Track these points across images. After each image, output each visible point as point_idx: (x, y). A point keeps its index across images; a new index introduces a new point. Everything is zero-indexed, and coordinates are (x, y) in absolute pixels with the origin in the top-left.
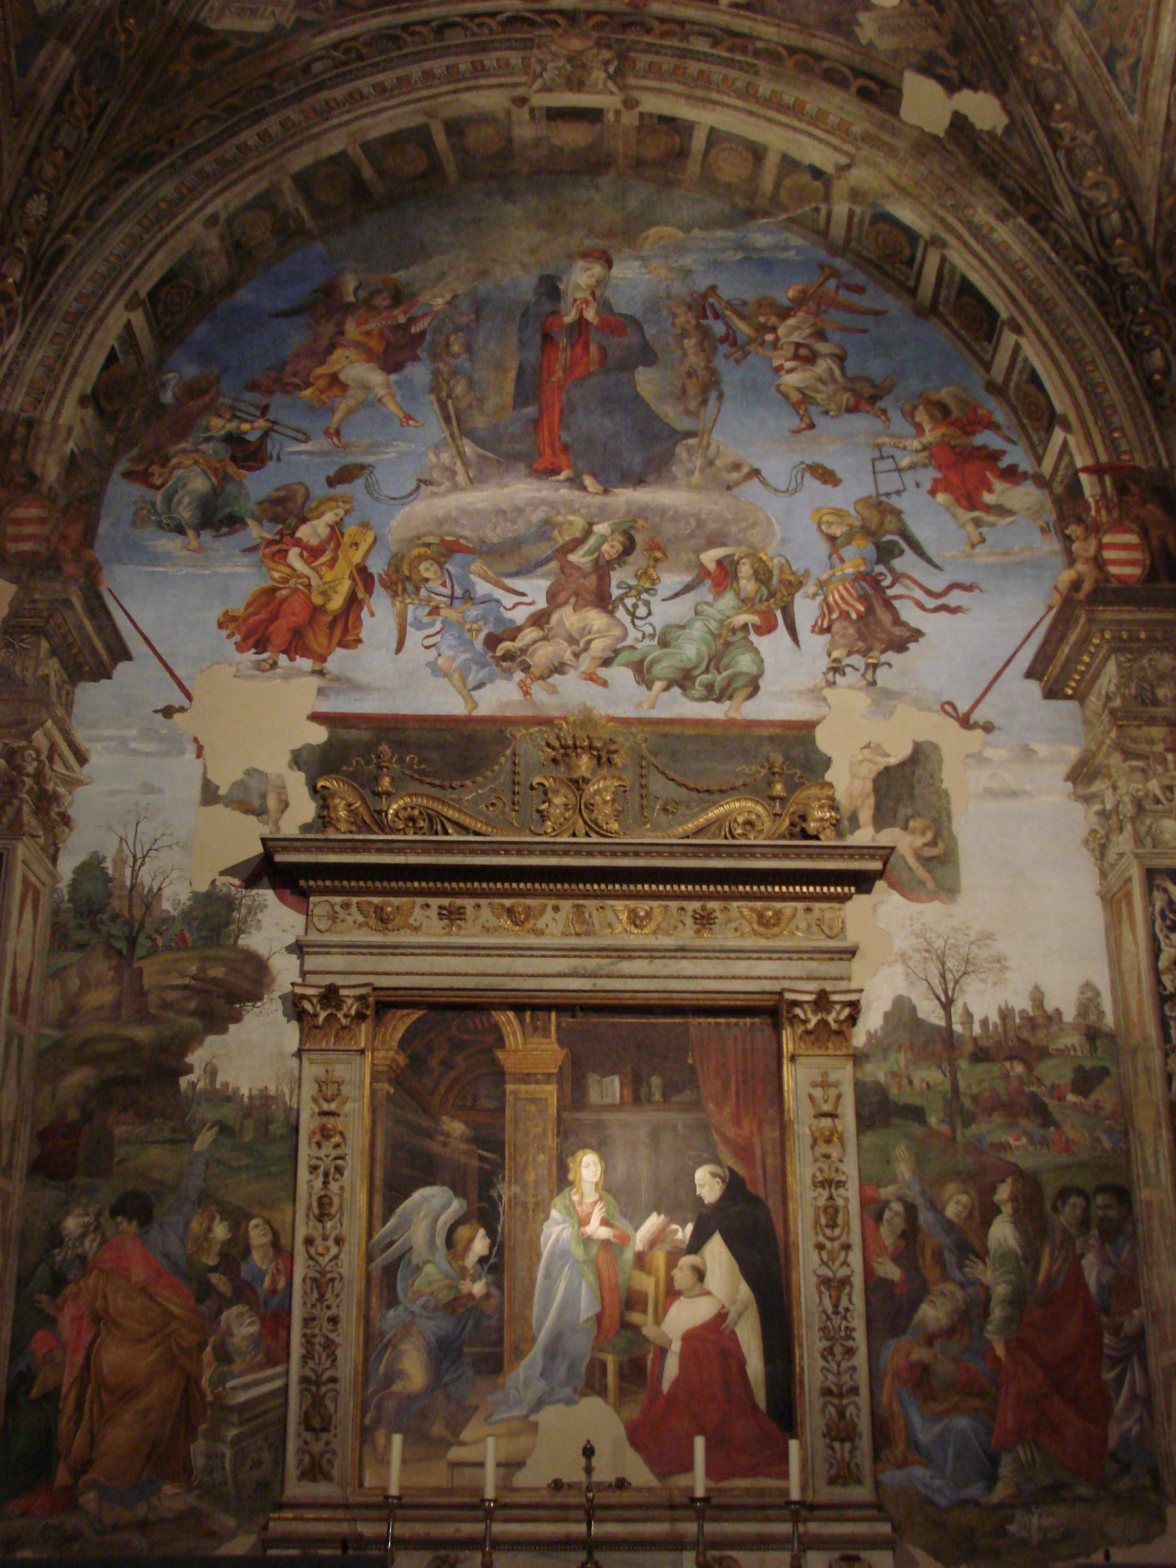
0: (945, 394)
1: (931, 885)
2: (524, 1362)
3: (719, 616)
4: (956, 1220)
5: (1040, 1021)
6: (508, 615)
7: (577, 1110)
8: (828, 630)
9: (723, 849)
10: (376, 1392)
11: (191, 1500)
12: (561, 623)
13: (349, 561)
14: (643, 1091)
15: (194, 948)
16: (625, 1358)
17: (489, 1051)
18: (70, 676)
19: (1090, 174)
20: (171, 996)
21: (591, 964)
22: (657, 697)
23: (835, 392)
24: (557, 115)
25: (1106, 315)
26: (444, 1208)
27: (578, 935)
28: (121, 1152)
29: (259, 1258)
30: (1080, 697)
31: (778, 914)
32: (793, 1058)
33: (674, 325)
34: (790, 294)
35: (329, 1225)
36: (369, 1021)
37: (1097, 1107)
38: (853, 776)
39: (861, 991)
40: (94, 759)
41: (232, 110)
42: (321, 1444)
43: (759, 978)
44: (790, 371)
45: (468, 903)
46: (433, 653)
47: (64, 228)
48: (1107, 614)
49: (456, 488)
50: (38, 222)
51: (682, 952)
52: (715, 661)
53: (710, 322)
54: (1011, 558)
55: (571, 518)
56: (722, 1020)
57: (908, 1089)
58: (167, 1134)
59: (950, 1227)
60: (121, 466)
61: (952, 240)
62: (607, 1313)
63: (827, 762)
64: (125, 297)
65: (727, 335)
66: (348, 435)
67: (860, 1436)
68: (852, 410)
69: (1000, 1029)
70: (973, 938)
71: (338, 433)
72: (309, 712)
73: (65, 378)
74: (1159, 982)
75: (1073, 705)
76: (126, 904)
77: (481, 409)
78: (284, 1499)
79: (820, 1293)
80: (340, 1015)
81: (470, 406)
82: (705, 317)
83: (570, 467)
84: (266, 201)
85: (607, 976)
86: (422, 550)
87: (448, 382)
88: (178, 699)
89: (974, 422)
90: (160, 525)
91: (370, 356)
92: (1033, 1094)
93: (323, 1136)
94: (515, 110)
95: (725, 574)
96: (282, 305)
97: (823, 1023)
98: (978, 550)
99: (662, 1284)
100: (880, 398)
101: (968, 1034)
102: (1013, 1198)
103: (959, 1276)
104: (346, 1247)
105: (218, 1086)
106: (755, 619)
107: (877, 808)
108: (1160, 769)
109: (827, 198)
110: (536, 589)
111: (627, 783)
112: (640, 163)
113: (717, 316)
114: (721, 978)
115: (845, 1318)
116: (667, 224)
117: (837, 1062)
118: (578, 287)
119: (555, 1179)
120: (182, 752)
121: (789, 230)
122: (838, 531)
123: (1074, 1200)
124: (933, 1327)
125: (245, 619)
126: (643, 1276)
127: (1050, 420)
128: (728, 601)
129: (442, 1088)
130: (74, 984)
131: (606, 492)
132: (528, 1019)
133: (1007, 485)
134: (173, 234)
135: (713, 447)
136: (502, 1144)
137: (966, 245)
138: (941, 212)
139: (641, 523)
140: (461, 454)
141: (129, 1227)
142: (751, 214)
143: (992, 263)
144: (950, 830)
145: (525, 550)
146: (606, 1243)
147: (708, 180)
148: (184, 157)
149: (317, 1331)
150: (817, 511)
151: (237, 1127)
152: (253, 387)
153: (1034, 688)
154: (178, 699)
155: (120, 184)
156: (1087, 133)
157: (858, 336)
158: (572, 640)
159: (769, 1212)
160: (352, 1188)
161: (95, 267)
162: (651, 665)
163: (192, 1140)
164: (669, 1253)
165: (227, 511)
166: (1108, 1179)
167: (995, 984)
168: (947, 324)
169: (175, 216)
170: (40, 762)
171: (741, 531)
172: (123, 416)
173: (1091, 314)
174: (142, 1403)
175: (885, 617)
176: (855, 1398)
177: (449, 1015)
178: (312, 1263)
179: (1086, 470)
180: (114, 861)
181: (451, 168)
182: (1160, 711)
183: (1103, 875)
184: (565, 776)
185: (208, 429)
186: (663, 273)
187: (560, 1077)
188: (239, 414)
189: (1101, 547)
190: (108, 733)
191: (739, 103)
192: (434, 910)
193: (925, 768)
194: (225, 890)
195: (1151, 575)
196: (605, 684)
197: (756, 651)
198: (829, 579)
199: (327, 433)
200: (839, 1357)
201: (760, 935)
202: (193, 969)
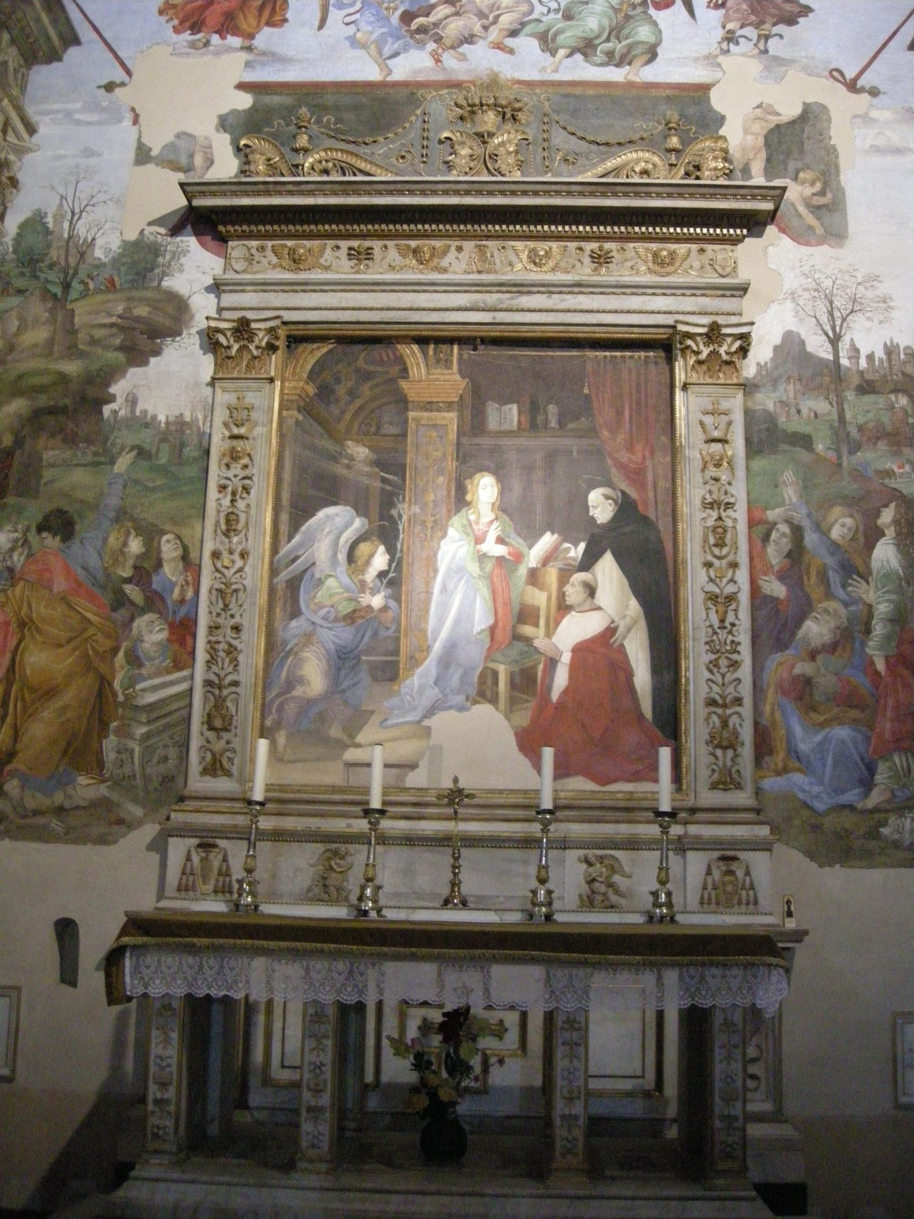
1: (819, 230)
2: (419, 671)
4: (840, 541)
7: (476, 435)
8: (723, 5)
9: (618, 188)
10: (278, 695)
11: (103, 790)
14: (540, 418)
15: (122, 290)
16: (516, 669)
17: (393, 380)
18: (26, 60)
20: (99, 333)
21: (492, 299)
22: (560, 63)
27: (479, 272)
28: (47, 474)
29: (171, 571)
31: (672, 255)
32: (685, 387)
35: (235, 539)
36: (279, 352)
38: (746, 132)
39: (752, 324)
40: (42, 130)
42: (222, 743)
43: (653, 312)
45: (376, 245)
46: (352, 28)
51: (578, 287)
52: (616, 32)
56: (618, 354)
57: (796, 417)
58: (89, 458)
59: (835, 547)
62: (500, 623)
67: (743, 744)
72: (236, 82)
76: (62, 252)
78: (186, 793)
79: (708, 609)
80: (252, 347)
85: (506, 310)
88: (119, 75)
93: (232, 458)
97: (714, 354)
99: (554, 598)
101: (854, 368)
102: (896, 522)
103: (841, 593)
104: (250, 561)
105: (138, 414)
107: (769, 160)
114: (616, 312)
115: (730, 632)
117: (729, 391)
119: (453, 500)
120: (120, 121)
124: (816, 643)
126: (536, 591)
129: (348, 416)
130: (13, 325)
132: (431, 352)
136: (403, 467)
141: (52, 541)
144: (838, 182)
146: (500, 560)
149: (221, 639)
151: (154, 450)
154: (120, 75)
158: (481, 15)
160: (258, 506)
162: (556, 35)
163: (112, 462)
164: (561, 570)
167: (881, 322)
174: (60, 702)
176: (738, 709)
177: (358, 348)
178: (218, 575)
180: (55, 217)
184: (474, 130)
190: (55, 107)
193: (814, 125)
194: (152, 238)
196: (511, 52)
197: (655, 24)
200: (724, 670)
202: (120, 309)
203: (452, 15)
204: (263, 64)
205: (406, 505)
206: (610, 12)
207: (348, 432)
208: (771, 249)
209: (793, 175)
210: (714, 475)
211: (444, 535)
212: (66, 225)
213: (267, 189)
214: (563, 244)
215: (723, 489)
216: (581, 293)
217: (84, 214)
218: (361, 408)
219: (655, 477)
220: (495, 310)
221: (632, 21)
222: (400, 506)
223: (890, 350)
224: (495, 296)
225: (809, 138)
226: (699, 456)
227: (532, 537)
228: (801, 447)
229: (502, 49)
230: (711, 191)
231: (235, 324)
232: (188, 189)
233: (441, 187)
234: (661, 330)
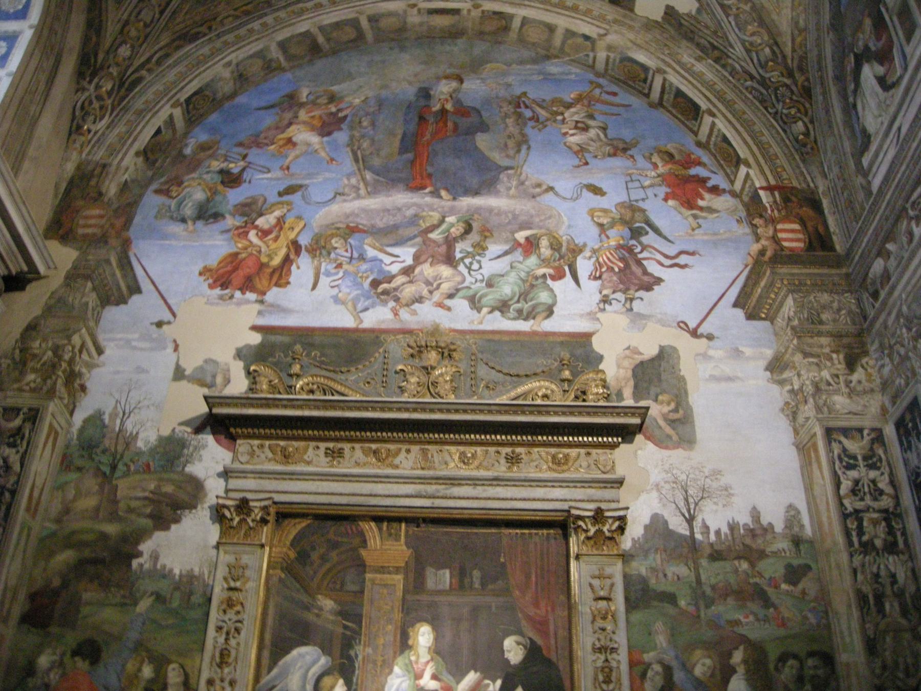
0: (670, 147)
1: (675, 438)
3: (527, 269)
4: (702, 678)
5: (759, 532)
6: (387, 268)
7: (417, 594)
8: (600, 277)
9: (526, 408)
12: (422, 273)
13: (287, 239)
14: (467, 581)
15: (155, 472)
17: (355, 550)
19: (750, 27)
20: (134, 504)
21: (431, 489)
22: (484, 317)
23: (601, 146)
25: (766, 108)
26: (315, 662)
27: (423, 469)
30: (771, 319)
31: (566, 457)
32: (577, 557)
33: (500, 112)
34: (572, 96)
36: (270, 525)
37: (804, 592)
38: (619, 366)
39: (627, 508)
40: (108, 352)
41: (247, 13)
44: (572, 135)
45: (346, 446)
46: (336, 291)
47: (142, 66)
48: (784, 270)
49: (359, 197)
51: (496, 481)
52: (524, 296)
53: (523, 110)
54: (719, 237)
55: (431, 213)
56: (526, 531)
57: (663, 580)
60: (155, 186)
61: (668, 69)
63: (600, 358)
68: (610, 155)
69: (730, 538)
70: (707, 474)
71: (288, 168)
72: (250, 325)
73: (129, 142)
74: (842, 504)
75: (767, 324)
80: (249, 520)
81: (371, 154)
82: (520, 107)
83: (432, 185)
84: (260, 54)
85: (442, 498)
86: (334, 231)
89: (689, 162)
90: (172, 218)
91: (313, 129)
92: (757, 584)
93: (228, 605)
94: (409, 9)
95: (531, 245)
96: (263, 104)
97: (599, 532)
98: (696, 232)
100: (630, 149)
101: (706, 541)
102: (745, 662)
106: (551, 271)
107: (636, 387)
108: (828, 364)
109: (593, 50)
110: (406, 254)
111: (462, 371)
113: (527, 107)
116: (498, 62)
118: (442, 93)
119: (398, 644)
120: (165, 348)
123: (791, 662)
125: (217, 270)
127: (738, 161)
128: (533, 260)
131: (454, 199)
133: (713, 196)
134: (204, 71)
136: (361, 616)
137: (678, 72)
138: (662, 57)
139: (476, 216)
140: (364, 179)
142: (548, 57)
143: (695, 82)
144: (687, 402)
145: (400, 231)
147: (522, 40)
151: (168, 596)
152: (240, 144)
153: (739, 313)
154: (167, 316)
155: (178, 48)
158: (428, 283)
159: (559, 671)
161: (159, 87)
162: (481, 298)
165: (213, 211)
166: (815, 647)
167: (724, 506)
168: (669, 111)
171: (541, 221)
172: (160, 161)
173: (757, 108)
175: (638, 271)
177: (329, 523)
179: (762, 188)
180: (110, 415)
181: (369, 36)
182: (823, 328)
183: (796, 432)
185: (209, 167)
187: (406, 570)
190: (119, 336)
191: (542, 6)
192: (322, 450)
193: (668, 362)
194: (180, 435)
195: (810, 247)
196: (449, 309)
197: (552, 290)
198: (600, 248)
199: (281, 168)
201: (554, 470)
202: (152, 487)
204: (271, 313)
205: (362, 647)
206: (520, 282)
207: (319, 588)
208: (639, 452)
209: (654, 398)
210: (601, 626)
211: (391, 671)
212: (118, 422)
214: (484, 448)
215: (608, 638)
216: (498, 485)
217: (132, 415)
218: (329, 570)
219: (556, 627)
220: (434, 497)
222: (356, 647)
223: (733, 527)
224: (434, 487)
226: (589, 610)
227: (459, 675)
228: (668, 602)
229: (442, 307)
230: (594, 410)
231: (237, 502)
232: (210, 400)
234: (559, 514)
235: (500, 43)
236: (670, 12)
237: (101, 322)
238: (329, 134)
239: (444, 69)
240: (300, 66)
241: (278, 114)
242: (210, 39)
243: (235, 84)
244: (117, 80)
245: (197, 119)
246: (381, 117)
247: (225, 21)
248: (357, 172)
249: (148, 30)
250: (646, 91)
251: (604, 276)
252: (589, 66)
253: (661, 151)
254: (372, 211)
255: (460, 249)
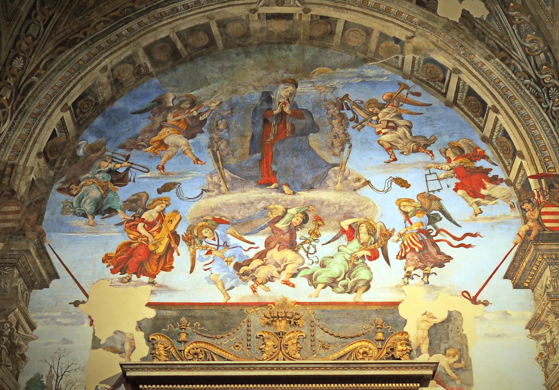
3: (350, 252)
8: (405, 257)
9: (351, 365)
12: (272, 257)
19: (529, 36)
22: (319, 292)
23: (407, 143)
24: (270, 17)
38: (418, 328)
40: (39, 328)
41: (116, 18)
47: (32, 74)
49: (220, 193)
50: (18, 71)
52: (348, 274)
54: (496, 221)
55: (277, 206)
60: (57, 186)
61: (463, 70)
64: (61, 106)
65: (354, 117)
66: (168, 169)
68: (414, 152)
71: (163, 168)
72: (146, 303)
77: (233, 155)
81: (228, 154)
82: (343, 109)
83: (276, 182)
84: (130, 60)
86: (204, 223)
87: (217, 143)
88: (82, 297)
90: (75, 213)
94: (251, 14)
96: (137, 108)
98: (479, 216)
100: (429, 145)
106: (368, 253)
107: (430, 344)
109: (402, 52)
112: (311, 38)
113: (348, 109)
116: (324, 66)
118: (281, 96)
120: (83, 323)
121: (383, 67)
122: (409, 209)
127: (515, 153)
128: (355, 244)
131: (294, 193)
134: (85, 75)
135: (347, 171)
137: (470, 72)
138: (458, 57)
140: (223, 177)
142: (365, 61)
143: (483, 80)
144: (468, 355)
145: (254, 222)
148: (92, 40)
150: (398, 200)
152: (123, 147)
154: (82, 297)
155: (60, 53)
156: (527, 16)
157: (418, 116)
158: (277, 265)
165: (108, 206)
169: (87, 67)
170: (12, 329)
172: (58, 162)
173: (533, 103)
180: (47, 377)
181: (220, 43)
186: (322, 89)
188: (115, 160)
189: (541, 214)
190: (46, 314)
191: (360, 9)
196: (293, 286)
197: (369, 269)
199: (158, 168)
203: (261, 265)
206: (346, 263)
212: (54, 382)
213: (167, 367)
217: (64, 376)
221: (356, 267)
225: (451, 331)
229: (288, 285)
232: (124, 367)
233: (259, 366)
235: (327, 47)
236: (466, 16)
237: (30, 303)
238: (193, 136)
239: (281, 74)
240: (164, 72)
241: (149, 118)
242: (86, 43)
243: (112, 89)
244: (14, 90)
245: (84, 123)
246: (234, 119)
247: (97, 27)
248: (218, 171)
249: (36, 42)
250: (444, 91)
251: (408, 256)
252: (398, 68)
253: (454, 147)
254: (231, 204)
255: (301, 235)
